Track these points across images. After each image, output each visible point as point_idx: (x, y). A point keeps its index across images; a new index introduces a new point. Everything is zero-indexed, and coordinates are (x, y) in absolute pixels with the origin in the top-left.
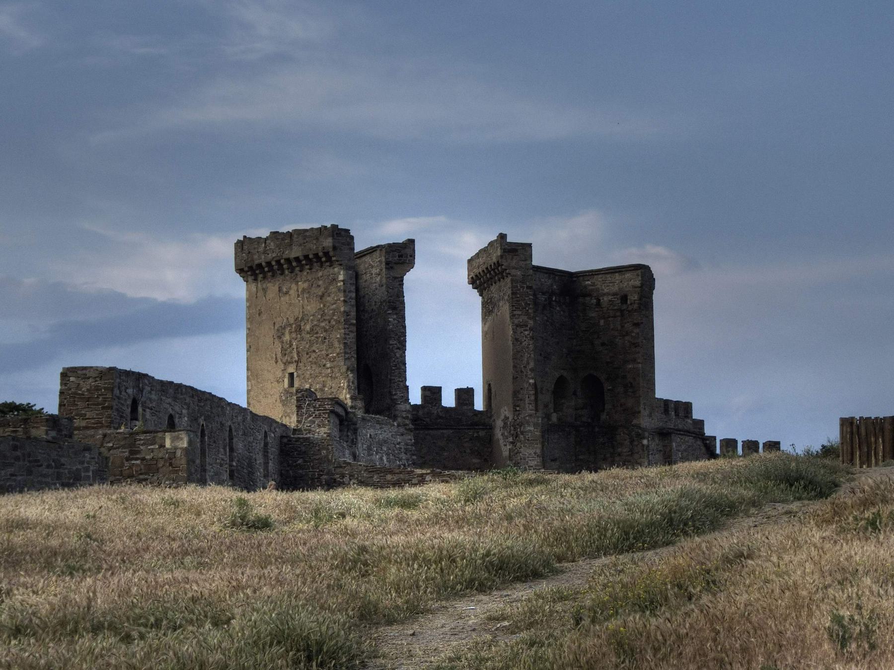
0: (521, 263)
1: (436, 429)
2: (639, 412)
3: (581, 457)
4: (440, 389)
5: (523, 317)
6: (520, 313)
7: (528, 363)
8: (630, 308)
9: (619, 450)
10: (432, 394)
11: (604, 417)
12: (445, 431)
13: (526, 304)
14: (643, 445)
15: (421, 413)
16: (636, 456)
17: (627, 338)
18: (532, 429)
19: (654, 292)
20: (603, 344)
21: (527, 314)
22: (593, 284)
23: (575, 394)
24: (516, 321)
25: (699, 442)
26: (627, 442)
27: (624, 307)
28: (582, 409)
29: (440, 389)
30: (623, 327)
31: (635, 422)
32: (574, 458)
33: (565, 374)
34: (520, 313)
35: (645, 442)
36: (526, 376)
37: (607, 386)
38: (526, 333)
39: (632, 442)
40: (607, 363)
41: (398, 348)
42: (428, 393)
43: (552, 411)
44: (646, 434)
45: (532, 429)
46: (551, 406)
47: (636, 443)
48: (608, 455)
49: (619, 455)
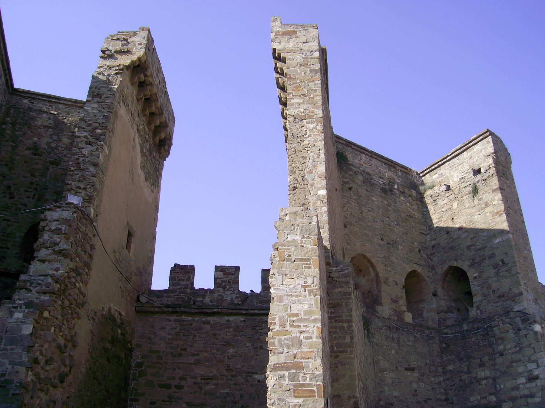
1: (218, 313)
2: (521, 294)
3: (450, 367)
4: (237, 269)
5: (305, 106)
6: (301, 101)
7: (315, 166)
8: (485, 178)
9: (501, 347)
10: (227, 275)
12: (232, 318)
13: (310, 90)
14: (536, 333)
15: (207, 300)
16: (528, 352)
18: (298, 238)
19: (512, 165)
21: (314, 104)
23: (435, 295)
27: (479, 177)
28: (446, 312)
29: (237, 269)
31: (516, 308)
32: (440, 369)
33: (419, 270)
34: (301, 101)
36: (312, 185)
37: (472, 274)
40: (469, 247)
41: (90, 144)
42: (221, 274)
43: (404, 308)
45: (298, 238)
46: (403, 302)
47: (523, 332)
49: (501, 354)
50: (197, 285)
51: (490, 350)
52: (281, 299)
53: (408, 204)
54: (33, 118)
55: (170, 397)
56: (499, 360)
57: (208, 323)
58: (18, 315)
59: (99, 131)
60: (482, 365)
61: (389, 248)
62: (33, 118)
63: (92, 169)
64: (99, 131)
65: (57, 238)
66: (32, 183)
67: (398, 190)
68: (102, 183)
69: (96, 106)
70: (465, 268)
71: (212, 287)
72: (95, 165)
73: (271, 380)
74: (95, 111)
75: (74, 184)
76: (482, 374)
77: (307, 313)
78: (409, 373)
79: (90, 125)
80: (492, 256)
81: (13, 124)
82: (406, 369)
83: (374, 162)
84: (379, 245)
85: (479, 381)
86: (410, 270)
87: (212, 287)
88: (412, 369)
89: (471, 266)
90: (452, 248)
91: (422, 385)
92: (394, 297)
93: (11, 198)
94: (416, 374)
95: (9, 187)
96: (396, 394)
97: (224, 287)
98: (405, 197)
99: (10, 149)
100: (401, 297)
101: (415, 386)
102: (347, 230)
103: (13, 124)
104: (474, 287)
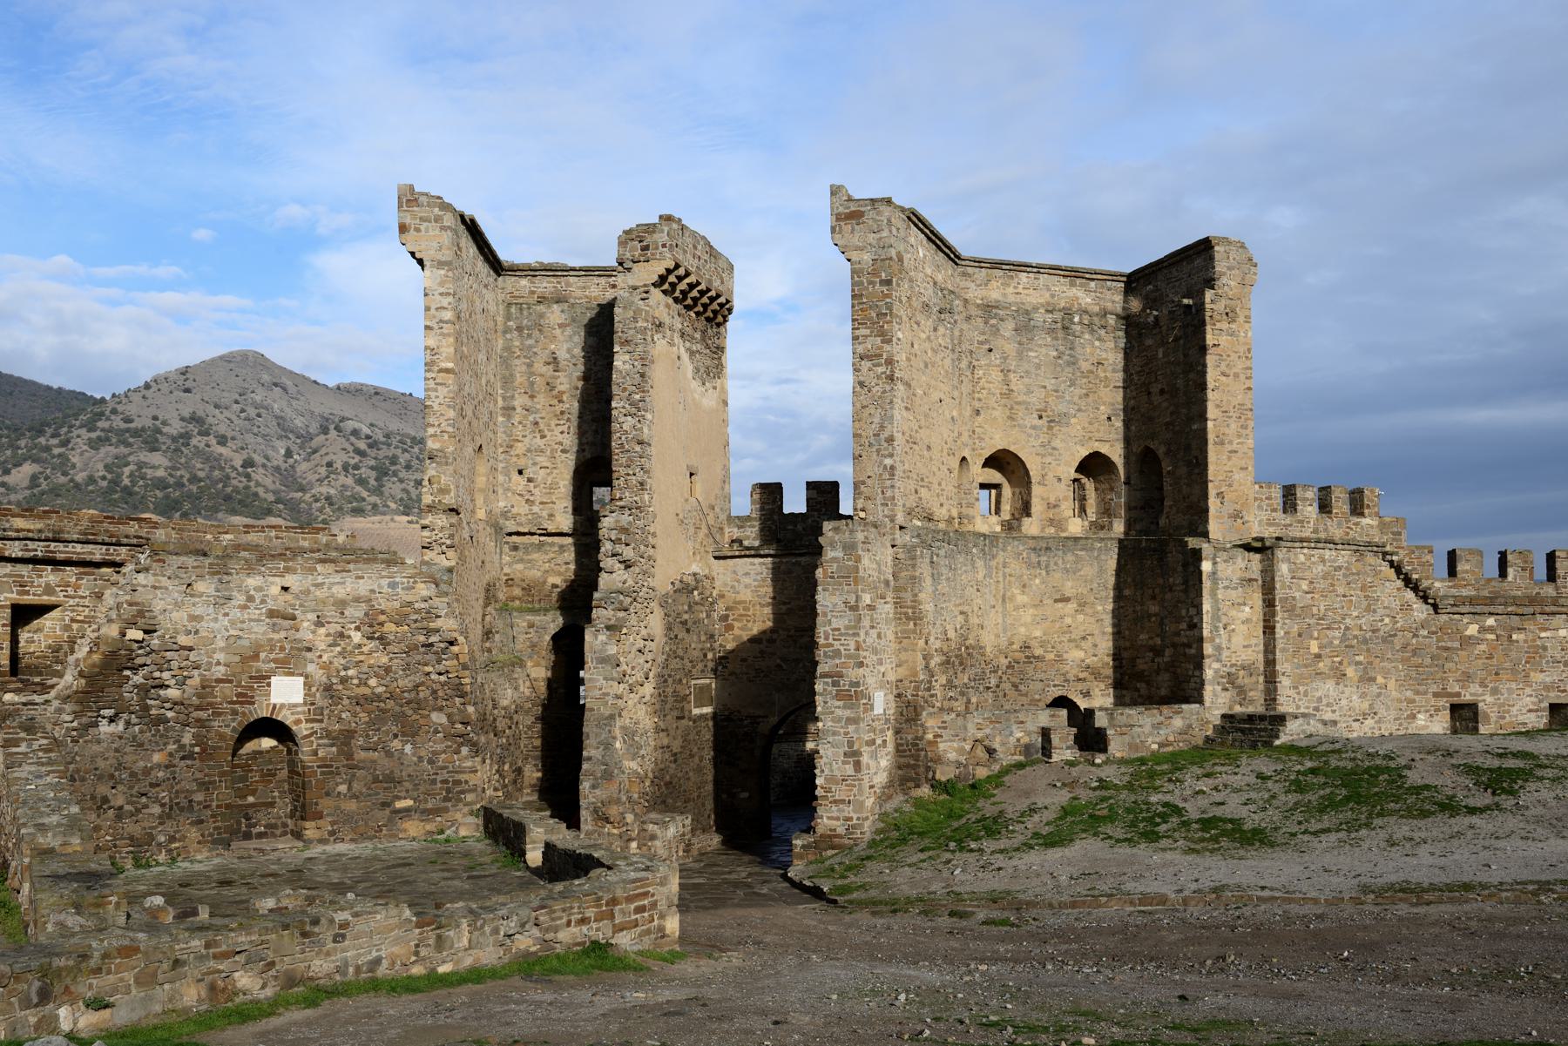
0: (872, 238)
11: (1162, 521)
15: (800, 527)
17: (1192, 376)
20: (1162, 392)
22: (1157, 289)
24: (860, 349)
25: (1371, 559)
26: (1180, 569)
30: (1185, 356)
35: (1206, 566)
37: (1167, 467)
38: (880, 370)
39: (1185, 565)
40: (1167, 424)
44: (1206, 548)
48: (1157, 591)
50: (786, 510)
51: (1161, 581)
52: (825, 614)
53: (1097, 343)
54: (542, 316)
55: (762, 652)
56: (1168, 596)
57: (798, 563)
58: (602, 638)
59: (637, 397)
60: (1153, 598)
61: (1050, 428)
62: (542, 316)
63: (638, 448)
64: (637, 397)
65: (619, 548)
66: (562, 413)
67: (1080, 323)
68: (649, 457)
69: (627, 357)
70: (1161, 451)
71: (803, 510)
72: (640, 443)
73: (818, 687)
74: (627, 366)
75: (623, 471)
76: (1154, 608)
77: (847, 628)
78: (1060, 605)
79: (625, 390)
80: (1188, 448)
81: (519, 329)
82: (1056, 601)
83: (1043, 279)
84: (1034, 427)
85: (1150, 616)
86: (1084, 453)
87: (803, 510)
88: (1067, 600)
89: (1167, 453)
90: (1151, 419)
91: (1081, 617)
92: (1052, 500)
93: (543, 437)
94: (1072, 606)
95: (536, 423)
96: (1038, 633)
97: (819, 511)
98: (1092, 332)
99: (524, 368)
100: (1066, 498)
101: (1068, 620)
102: (980, 419)
103: (519, 329)
104: (1167, 488)
